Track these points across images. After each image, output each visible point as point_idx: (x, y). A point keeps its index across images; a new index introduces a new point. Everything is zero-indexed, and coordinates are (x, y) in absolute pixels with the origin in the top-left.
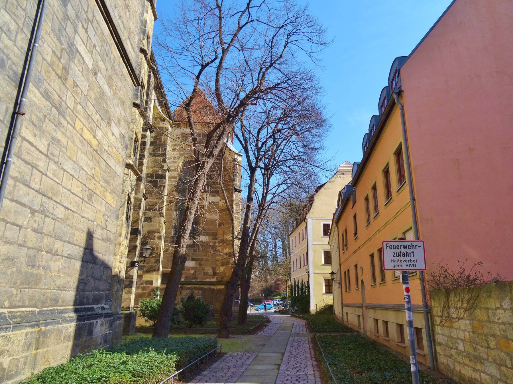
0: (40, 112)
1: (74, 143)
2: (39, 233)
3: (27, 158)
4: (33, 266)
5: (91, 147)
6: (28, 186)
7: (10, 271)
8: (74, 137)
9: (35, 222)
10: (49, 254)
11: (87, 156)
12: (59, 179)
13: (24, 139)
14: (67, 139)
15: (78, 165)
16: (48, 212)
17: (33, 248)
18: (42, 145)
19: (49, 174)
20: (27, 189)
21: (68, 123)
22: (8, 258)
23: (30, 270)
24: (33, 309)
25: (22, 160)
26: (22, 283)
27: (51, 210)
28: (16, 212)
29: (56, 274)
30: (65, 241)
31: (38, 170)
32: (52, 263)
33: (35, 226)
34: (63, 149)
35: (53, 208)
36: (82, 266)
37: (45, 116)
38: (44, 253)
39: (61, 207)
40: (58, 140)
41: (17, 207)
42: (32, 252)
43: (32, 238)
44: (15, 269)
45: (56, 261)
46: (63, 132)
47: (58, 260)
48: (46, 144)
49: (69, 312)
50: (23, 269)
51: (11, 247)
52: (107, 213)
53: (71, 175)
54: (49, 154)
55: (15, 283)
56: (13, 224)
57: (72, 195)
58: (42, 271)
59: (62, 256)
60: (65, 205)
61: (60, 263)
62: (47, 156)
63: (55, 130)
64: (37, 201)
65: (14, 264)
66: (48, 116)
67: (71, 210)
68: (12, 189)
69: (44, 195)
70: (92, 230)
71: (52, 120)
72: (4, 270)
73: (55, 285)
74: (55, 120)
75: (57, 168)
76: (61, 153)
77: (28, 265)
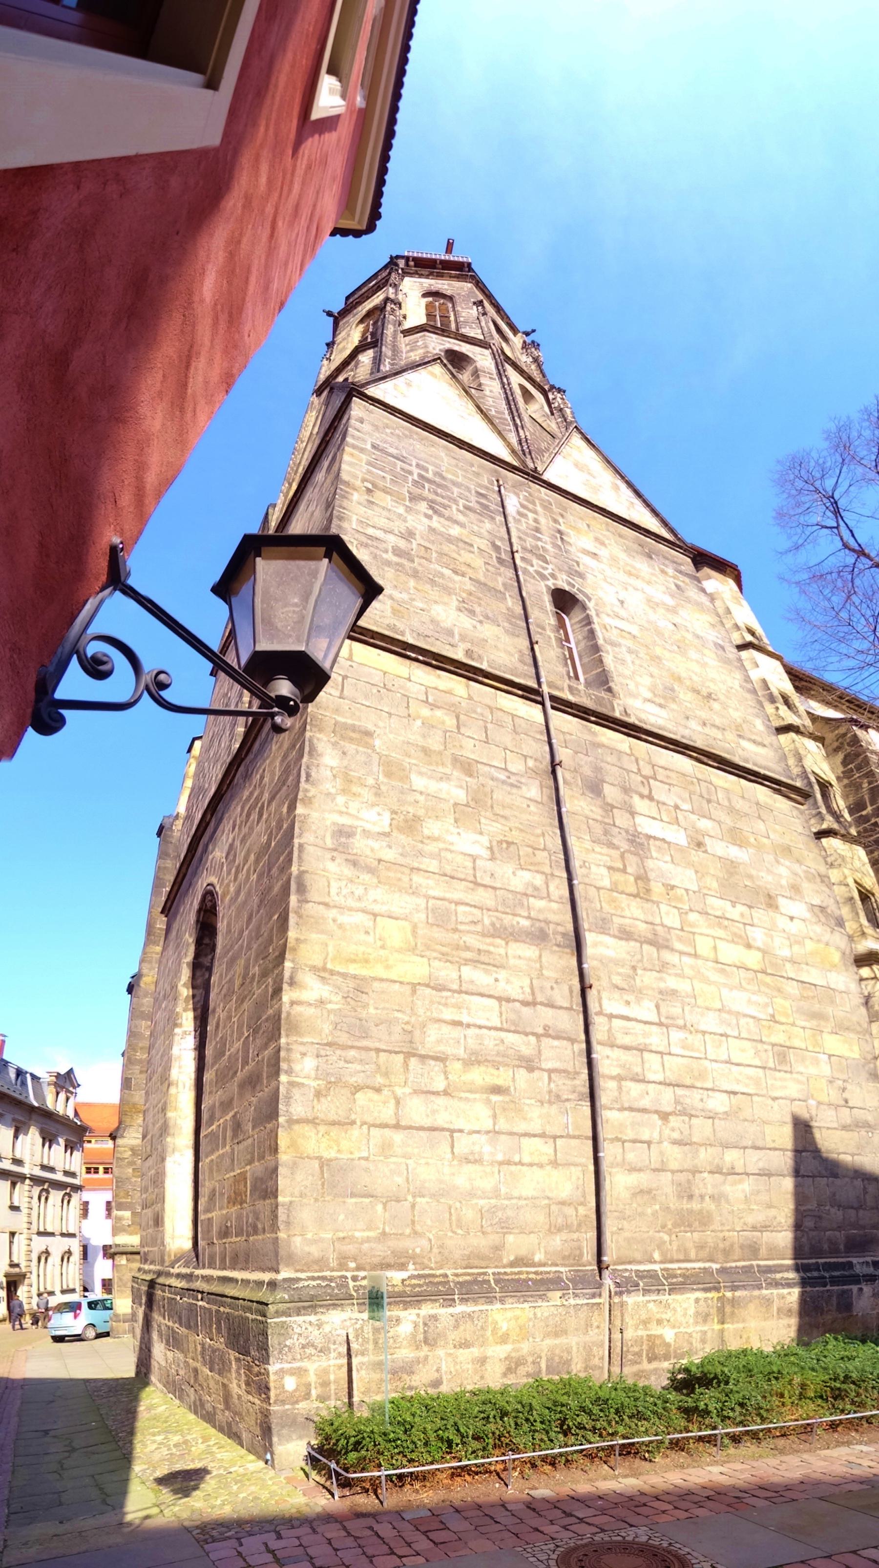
0: (623, 966)
1: (707, 981)
2: (686, 1145)
3: (627, 1040)
4: (691, 1197)
5: (748, 969)
6: (643, 1081)
7: (649, 1211)
8: (702, 970)
9: (673, 1130)
10: (717, 1175)
11: (745, 990)
12: (698, 1050)
13: (611, 1016)
14: (688, 981)
15: (730, 1012)
16: (693, 1108)
17: (681, 1171)
18: (646, 1010)
19: (674, 1050)
20: (642, 1086)
21: (681, 953)
22: (642, 1191)
23: (686, 1205)
24: (707, 1265)
26: (675, 1225)
27: (700, 1105)
29: (742, 1207)
31: (651, 1051)
32: (728, 1189)
33: (676, 1135)
34: (687, 1000)
35: (702, 1100)
36: (797, 1186)
37: (634, 968)
38: (706, 1175)
39: (717, 1094)
40: (673, 990)
42: (682, 1177)
43: (675, 1156)
44: (657, 1207)
45: (734, 1184)
46: (676, 975)
47: (741, 1182)
48: (652, 1006)
49: (787, 1271)
50: (671, 1205)
51: (642, 1174)
53: (722, 1035)
54: (663, 1020)
55: (664, 1226)
56: (634, 1141)
57: (734, 1068)
58: (709, 1205)
59: (748, 1174)
60: (724, 1088)
61: (746, 1186)
62: (660, 1024)
63: (661, 979)
64: (666, 1098)
65: (654, 1198)
66: (640, 965)
68: (616, 1094)
69: (678, 1086)
70: (805, 1115)
71: (649, 967)
72: (639, 1210)
73: (745, 1224)
74: (654, 965)
75: (688, 1035)
76: (687, 1008)
77: (680, 1197)
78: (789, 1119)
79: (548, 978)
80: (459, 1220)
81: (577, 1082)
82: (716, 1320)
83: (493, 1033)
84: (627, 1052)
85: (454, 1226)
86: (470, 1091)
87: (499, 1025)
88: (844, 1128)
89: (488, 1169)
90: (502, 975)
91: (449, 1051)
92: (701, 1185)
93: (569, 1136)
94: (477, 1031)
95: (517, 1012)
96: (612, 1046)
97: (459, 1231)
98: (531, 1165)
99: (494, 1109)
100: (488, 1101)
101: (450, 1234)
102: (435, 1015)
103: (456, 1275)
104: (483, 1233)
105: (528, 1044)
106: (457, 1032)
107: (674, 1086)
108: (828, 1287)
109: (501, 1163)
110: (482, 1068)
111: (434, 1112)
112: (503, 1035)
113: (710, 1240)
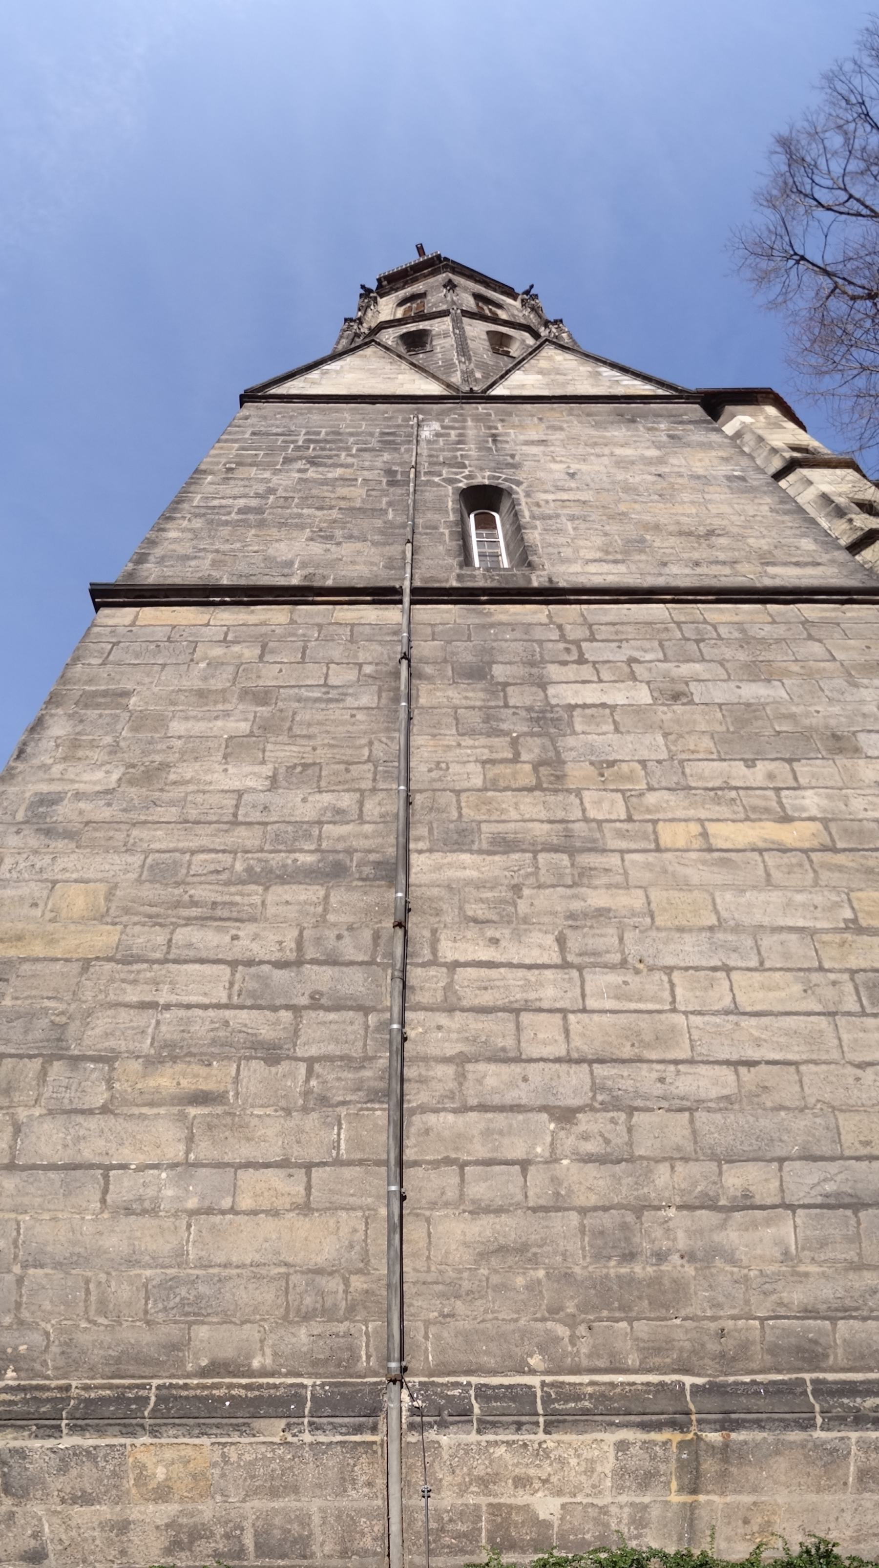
3: (486, 999)
6: (518, 1060)
19: (591, 1003)
20: (517, 1069)
25: (463, 1010)
28: (487, 1133)
33: (591, 1147)
38: (672, 1212)
40: (598, 910)
41: (491, 1121)
42: (607, 1220)
48: (549, 940)
54: (570, 958)
62: (565, 965)
63: (575, 897)
68: (452, 1085)
79: (335, 925)
80: (103, 1302)
81: (367, 1073)
83: (211, 1013)
85: (92, 1313)
86: (151, 1104)
87: (224, 1000)
89: (168, 1223)
90: (246, 931)
91: (122, 1045)
92: (658, 1233)
93: (338, 1162)
94: (182, 1013)
95: (264, 980)
96: (451, 1010)
97: (101, 1320)
98: (254, 1213)
99: (190, 1128)
100: (182, 1117)
101: (84, 1324)
102: (112, 997)
103: (86, 1388)
104: (148, 1323)
105: (277, 1022)
106: (148, 1018)
107: (590, 1062)
109: (192, 1213)
110: (180, 1067)
111: (78, 1139)
112: (228, 1014)
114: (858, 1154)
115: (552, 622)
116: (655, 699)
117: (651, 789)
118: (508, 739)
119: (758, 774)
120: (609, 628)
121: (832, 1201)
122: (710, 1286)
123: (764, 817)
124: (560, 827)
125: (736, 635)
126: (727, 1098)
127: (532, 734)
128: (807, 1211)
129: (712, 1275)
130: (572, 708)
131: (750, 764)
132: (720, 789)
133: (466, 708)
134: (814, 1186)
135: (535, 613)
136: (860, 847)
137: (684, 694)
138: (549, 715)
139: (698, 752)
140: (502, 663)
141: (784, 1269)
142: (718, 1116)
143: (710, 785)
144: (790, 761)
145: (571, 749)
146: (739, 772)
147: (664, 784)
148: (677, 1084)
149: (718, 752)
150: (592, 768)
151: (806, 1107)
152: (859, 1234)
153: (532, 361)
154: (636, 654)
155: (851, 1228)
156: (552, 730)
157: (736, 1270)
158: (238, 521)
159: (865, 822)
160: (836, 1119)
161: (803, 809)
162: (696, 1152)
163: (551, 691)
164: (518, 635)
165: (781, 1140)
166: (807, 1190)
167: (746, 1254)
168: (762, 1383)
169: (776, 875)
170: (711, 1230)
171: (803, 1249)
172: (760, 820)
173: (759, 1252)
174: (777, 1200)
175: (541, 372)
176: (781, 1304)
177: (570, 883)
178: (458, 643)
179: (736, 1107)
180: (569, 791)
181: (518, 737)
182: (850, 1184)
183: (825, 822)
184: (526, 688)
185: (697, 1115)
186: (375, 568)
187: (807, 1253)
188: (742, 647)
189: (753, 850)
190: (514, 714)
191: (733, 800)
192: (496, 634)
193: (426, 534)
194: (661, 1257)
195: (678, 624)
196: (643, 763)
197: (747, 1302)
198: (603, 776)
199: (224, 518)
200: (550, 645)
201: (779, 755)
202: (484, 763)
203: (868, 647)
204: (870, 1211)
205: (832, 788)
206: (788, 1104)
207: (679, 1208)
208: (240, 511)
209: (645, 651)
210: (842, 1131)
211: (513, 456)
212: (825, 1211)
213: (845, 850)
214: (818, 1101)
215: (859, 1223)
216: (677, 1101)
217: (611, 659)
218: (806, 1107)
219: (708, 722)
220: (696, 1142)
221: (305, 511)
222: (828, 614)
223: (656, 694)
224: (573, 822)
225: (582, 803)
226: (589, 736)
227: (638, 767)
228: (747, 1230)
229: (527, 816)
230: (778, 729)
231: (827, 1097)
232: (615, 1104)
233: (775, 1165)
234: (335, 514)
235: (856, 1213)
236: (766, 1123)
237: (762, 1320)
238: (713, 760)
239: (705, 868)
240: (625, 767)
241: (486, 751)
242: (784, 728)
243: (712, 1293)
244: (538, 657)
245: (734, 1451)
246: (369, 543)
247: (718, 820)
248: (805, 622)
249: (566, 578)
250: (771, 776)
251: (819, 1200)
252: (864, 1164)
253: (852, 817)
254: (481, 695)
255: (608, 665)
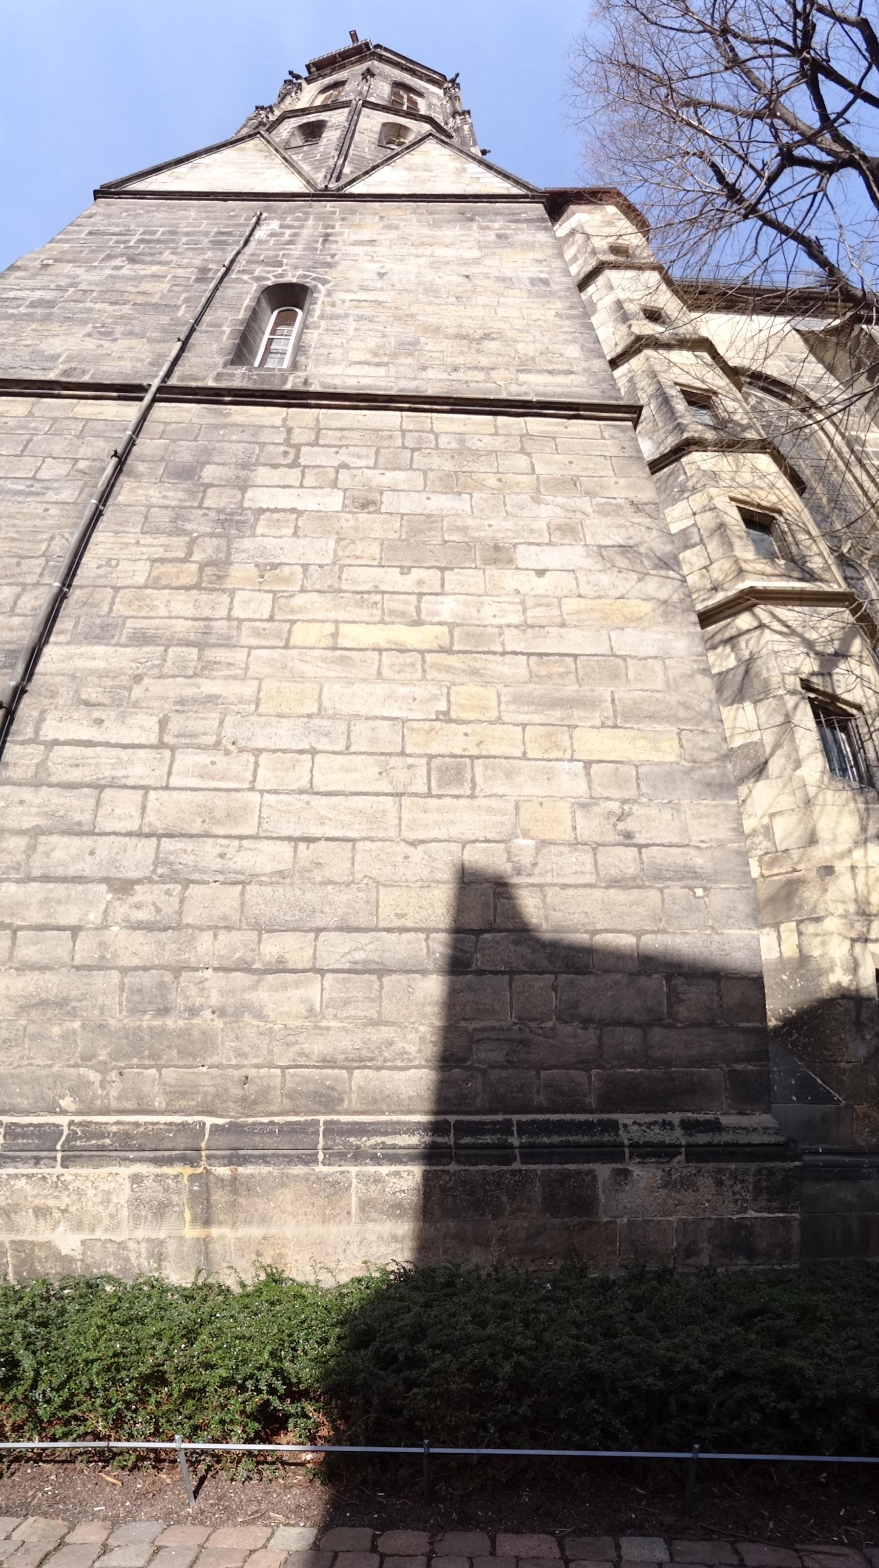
4: (164, 1011)
7: (56, 1031)
23: (147, 1021)
26: (116, 1055)
30: (318, 931)
44: (77, 1024)
50: (112, 1022)
52: (598, 791)
67: (328, 839)
78: (446, 874)
82: (188, 1215)
84: (66, 793)
88: (616, 883)
108: (516, 1165)
113: (205, 1081)
114: (392, 925)
115: (284, 425)
116: (344, 506)
117: (303, 590)
118: (187, 539)
119: (408, 582)
120: (338, 434)
121: (359, 967)
122: (237, 1037)
123: (397, 620)
124: (201, 624)
125: (454, 445)
126: (280, 873)
127: (211, 535)
128: (335, 975)
129: (239, 1027)
130: (262, 511)
131: (405, 570)
132: (368, 592)
133: (160, 507)
134: (345, 954)
135: (273, 415)
136: (474, 649)
137: (373, 503)
138: (237, 518)
139: (361, 558)
140: (216, 464)
141: (307, 1024)
142: (269, 889)
143: (359, 589)
144: (442, 569)
145: (243, 551)
146: (392, 578)
147: (317, 587)
148: (236, 859)
149: (381, 558)
150: (256, 570)
151: (353, 882)
152: (380, 997)
153: (407, 156)
154: (349, 460)
155: (374, 992)
156: (233, 532)
157: (262, 1024)
158: (24, 314)
159: (489, 628)
160: (378, 893)
161: (437, 614)
162: (241, 921)
163: (250, 494)
164: (245, 436)
165: (322, 912)
166: (338, 957)
167: (274, 1010)
168: (278, 1124)
169: (386, 673)
170: (244, 991)
171: (327, 1007)
172: (393, 623)
173: (286, 1008)
174: (308, 966)
175: (409, 169)
176: (302, 1054)
177: (191, 674)
178: (183, 443)
179: (288, 881)
180: (224, 591)
181: (197, 537)
182: (378, 953)
183: (452, 626)
184: (228, 490)
185: (248, 887)
186: (139, 365)
187: (331, 1010)
188: (453, 457)
189: (374, 649)
190: (205, 515)
191: (376, 603)
192: (223, 435)
193: (207, 332)
194: (193, 1012)
195: (403, 432)
196: (305, 567)
197: (270, 1052)
198: (262, 577)
199: (10, 311)
200: (271, 448)
201: (436, 564)
202: (155, 561)
203: (571, 462)
204: (394, 976)
205: (472, 595)
206: (336, 879)
207: (216, 969)
208: (33, 305)
209: (359, 457)
210: (381, 904)
211: (333, 256)
212: (352, 975)
213: (459, 652)
214: (366, 876)
215: (382, 987)
216: (232, 875)
217: (323, 464)
218: (353, 882)
219: (384, 531)
220: (242, 912)
221: (98, 306)
222: (550, 428)
223: (347, 502)
224: (217, 620)
225: (232, 602)
226: (266, 539)
227: (299, 569)
228: (277, 991)
229: (174, 614)
230: (446, 538)
231: (374, 874)
232: (174, 877)
233: (312, 935)
234: (126, 309)
235: (380, 979)
236: (312, 897)
237: (283, 1068)
238: (372, 566)
239: (323, 665)
240: (287, 570)
241: (161, 550)
242: (452, 538)
243: (238, 1044)
244: (254, 460)
245: (242, 1184)
246: (145, 340)
247: (354, 622)
248: (525, 436)
249: (322, 379)
250: (420, 582)
251: (347, 966)
252: (394, 936)
253: (479, 623)
254: (181, 495)
255: (316, 470)
